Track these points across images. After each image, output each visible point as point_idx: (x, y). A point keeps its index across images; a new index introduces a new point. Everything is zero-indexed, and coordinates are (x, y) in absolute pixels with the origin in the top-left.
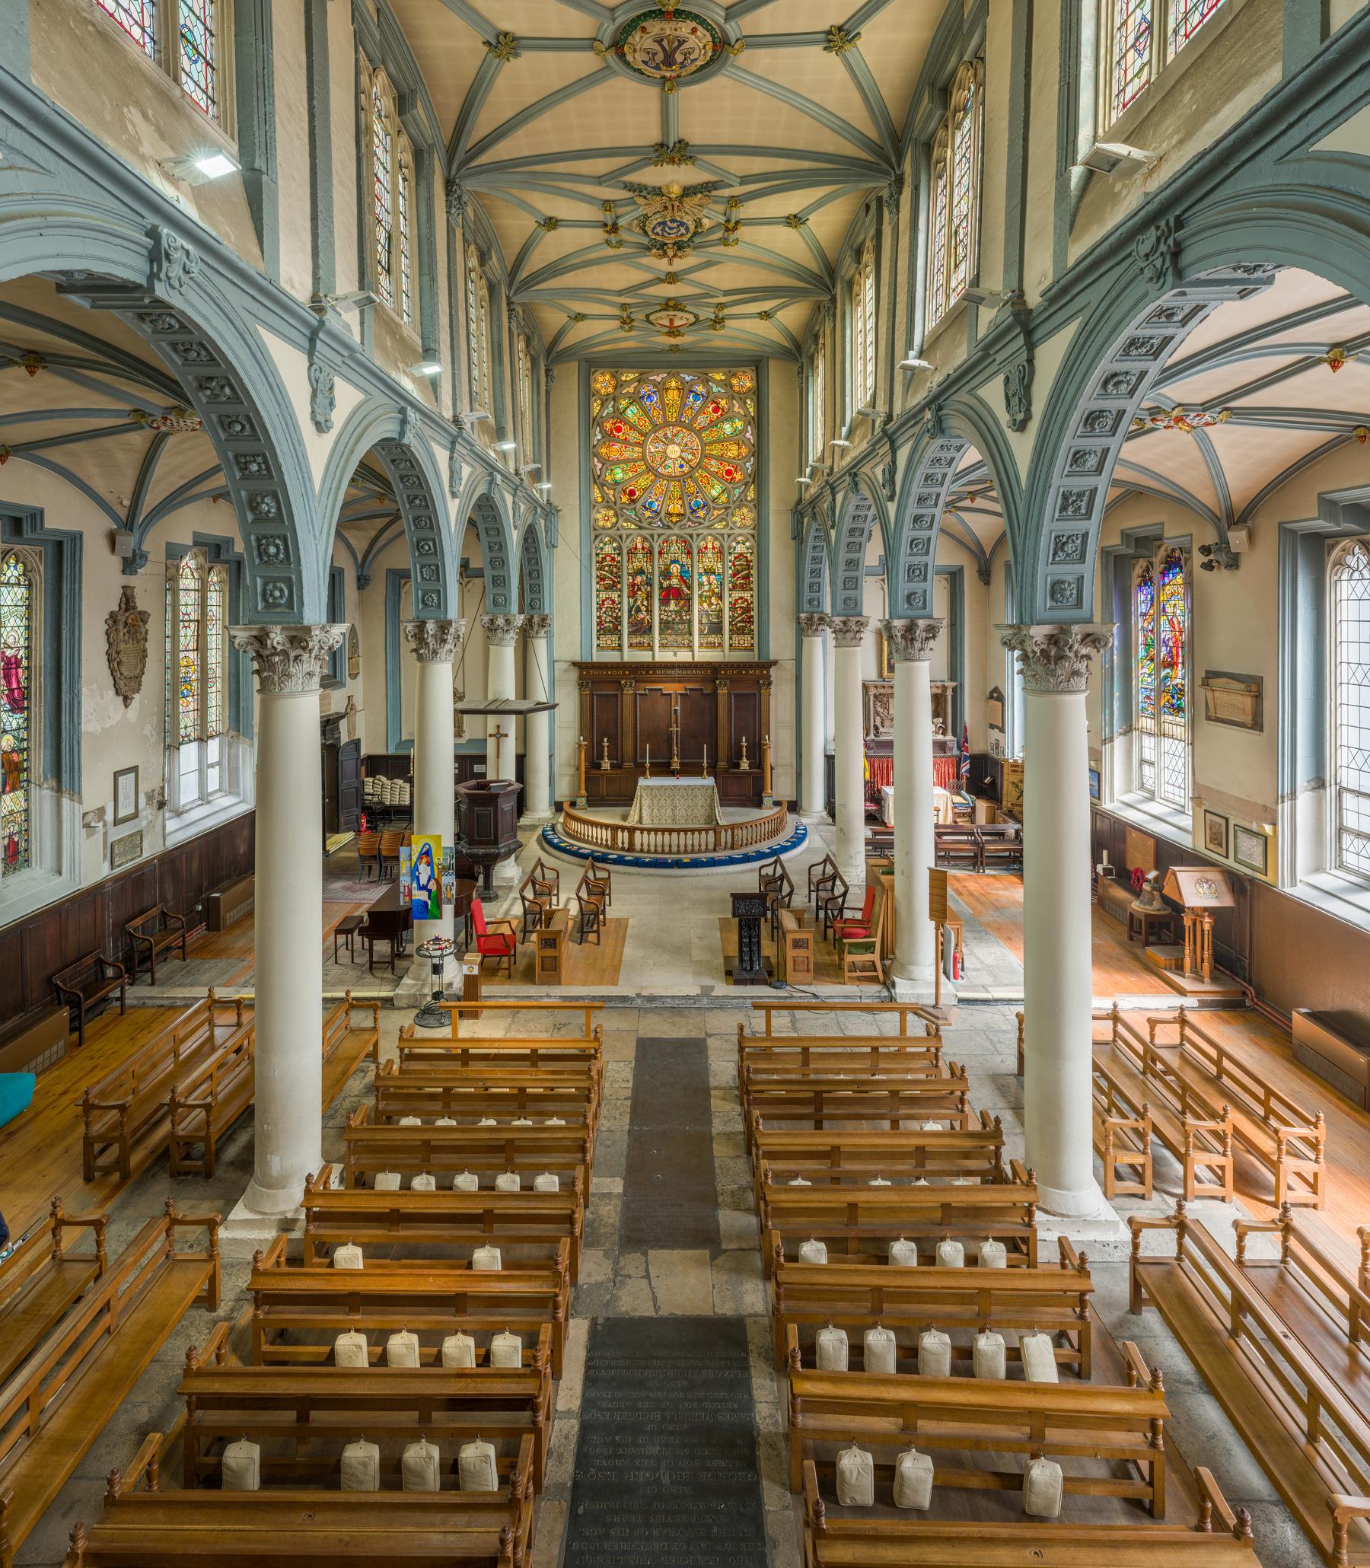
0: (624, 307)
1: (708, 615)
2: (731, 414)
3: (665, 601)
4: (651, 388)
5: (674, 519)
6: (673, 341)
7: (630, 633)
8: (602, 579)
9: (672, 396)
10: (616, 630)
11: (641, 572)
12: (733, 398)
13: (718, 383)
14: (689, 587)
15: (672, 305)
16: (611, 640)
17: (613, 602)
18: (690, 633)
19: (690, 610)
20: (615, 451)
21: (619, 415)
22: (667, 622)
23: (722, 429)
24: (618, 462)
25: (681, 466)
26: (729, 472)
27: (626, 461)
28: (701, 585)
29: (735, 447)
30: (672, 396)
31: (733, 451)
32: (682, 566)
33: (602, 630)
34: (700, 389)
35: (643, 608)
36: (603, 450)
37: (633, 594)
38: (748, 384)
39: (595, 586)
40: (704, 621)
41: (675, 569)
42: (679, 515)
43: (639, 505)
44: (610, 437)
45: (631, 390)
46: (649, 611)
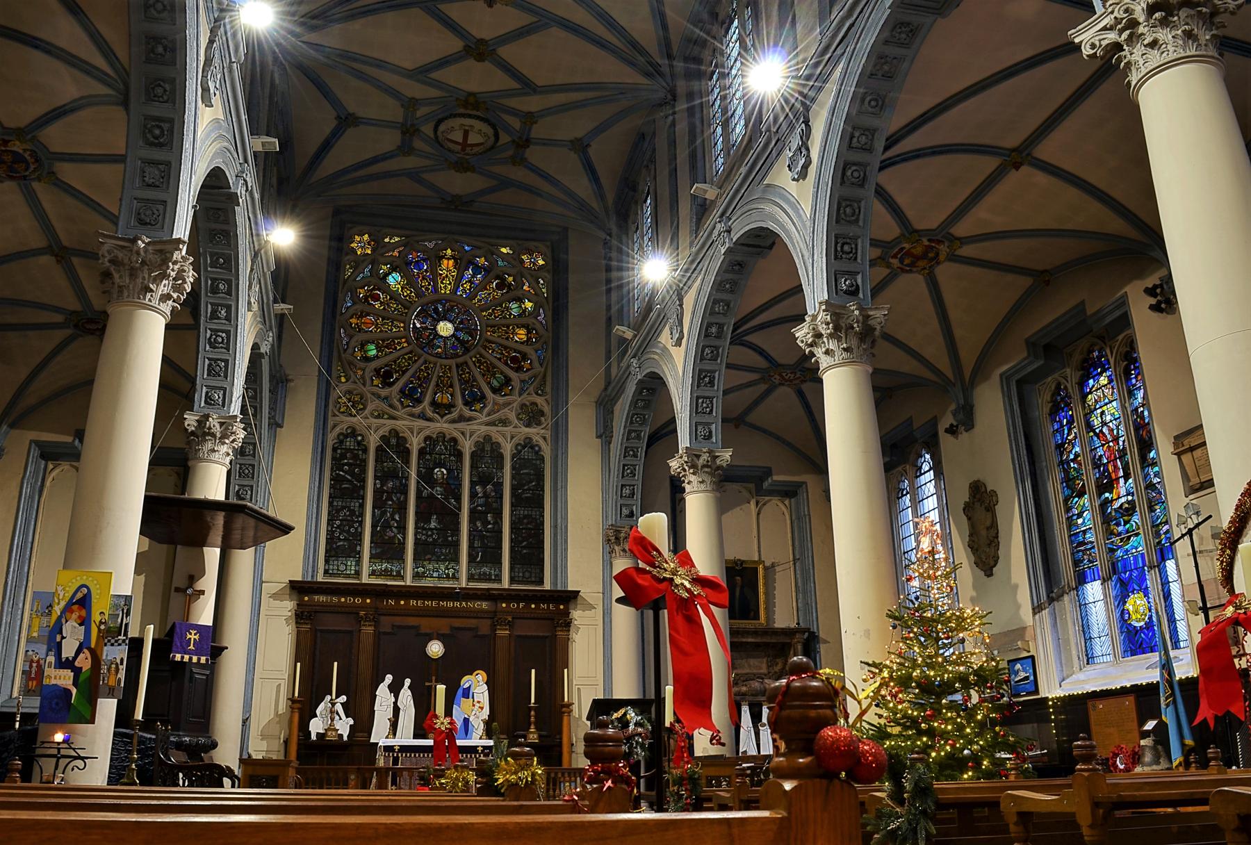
0: (411, 104)
1: (482, 538)
2: (519, 293)
3: (422, 517)
6: (460, 184)
7: (372, 557)
12: (522, 276)
14: (458, 499)
15: (472, 104)
17: (352, 512)
22: (426, 543)
23: (508, 309)
26: (514, 359)
28: (473, 495)
31: (521, 334)
34: (481, 261)
36: (354, 321)
38: (541, 262)
41: (440, 472)
42: (450, 407)
45: (396, 253)
46: (402, 528)
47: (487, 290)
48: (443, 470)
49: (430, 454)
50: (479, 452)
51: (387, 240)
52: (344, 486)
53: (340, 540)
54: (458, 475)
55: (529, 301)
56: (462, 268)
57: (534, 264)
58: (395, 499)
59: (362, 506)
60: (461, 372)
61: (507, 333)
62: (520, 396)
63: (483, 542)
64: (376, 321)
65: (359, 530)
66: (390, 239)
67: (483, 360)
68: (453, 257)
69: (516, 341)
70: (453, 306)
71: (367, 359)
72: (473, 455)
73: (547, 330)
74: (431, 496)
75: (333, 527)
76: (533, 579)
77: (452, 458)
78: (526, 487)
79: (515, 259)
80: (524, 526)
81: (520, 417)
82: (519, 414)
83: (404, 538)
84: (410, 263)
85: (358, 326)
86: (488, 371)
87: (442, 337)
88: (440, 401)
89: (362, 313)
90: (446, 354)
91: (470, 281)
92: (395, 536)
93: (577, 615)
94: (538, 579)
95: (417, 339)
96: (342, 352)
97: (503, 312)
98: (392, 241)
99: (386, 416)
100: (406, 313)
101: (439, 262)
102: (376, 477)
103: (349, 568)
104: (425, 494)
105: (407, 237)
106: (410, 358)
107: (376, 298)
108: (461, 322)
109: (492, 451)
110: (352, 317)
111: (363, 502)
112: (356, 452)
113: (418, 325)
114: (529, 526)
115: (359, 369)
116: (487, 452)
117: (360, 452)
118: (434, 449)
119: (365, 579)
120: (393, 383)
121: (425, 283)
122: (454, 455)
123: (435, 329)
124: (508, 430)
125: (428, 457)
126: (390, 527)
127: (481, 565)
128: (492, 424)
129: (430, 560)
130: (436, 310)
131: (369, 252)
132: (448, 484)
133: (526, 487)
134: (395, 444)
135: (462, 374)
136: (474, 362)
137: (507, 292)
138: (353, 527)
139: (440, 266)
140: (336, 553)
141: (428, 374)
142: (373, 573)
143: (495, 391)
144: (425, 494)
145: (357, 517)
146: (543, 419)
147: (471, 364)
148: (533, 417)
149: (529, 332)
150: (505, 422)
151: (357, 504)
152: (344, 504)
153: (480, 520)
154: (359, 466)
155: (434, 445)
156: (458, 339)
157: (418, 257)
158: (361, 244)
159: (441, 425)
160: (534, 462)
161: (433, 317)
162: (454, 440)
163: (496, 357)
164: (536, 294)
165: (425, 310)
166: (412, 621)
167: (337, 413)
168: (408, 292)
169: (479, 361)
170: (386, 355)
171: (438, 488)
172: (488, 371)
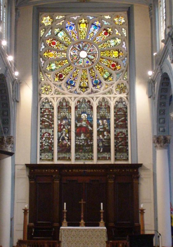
1: (103, 142)
2: (114, 36)
3: (78, 134)
4: (72, 23)
7: (58, 152)
8: (43, 122)
9: (83, 27)
10: (50, 150)
11: (65, 118)
13: (107, 20)
14: (92, 126)
16: (46, 155)
17: (50, 134)
18: (92, 151)
19: (92, 140)
20: (52, 55)
21: (55, 37)
22: (79, 146)
23: (109, 43)
24: (52, 61)
25: (87, 62)
26: (113, 65)
27: (58, 60)
28: (98, 125)
29: (117, 52)
30: (83, 27)
31: (115, 54)
32: (88, 115)
33: (43, 151)
34: (97, 23)
35: (66, 138)
36: (45, 54)
37: (60, 130)
38: (123, 21)
39: (39, 126)
40: (101, 145)
41: (84, 116)
42: (87, 88)
43: (64, 82)
44: (49, 49)
45: (61, 24)
46: (69, 139)
47: (100, 35)
48: (85, 115)
49: (80, 108)
50: (100, 106)
51: (57, 18)
52: (45, 124)
53: (45, 146)
54: (91, 116)
55: (119, 39)
56: (89, 27)
57: (120, 22)
58: (66, 128)
59: (53, 131)
60: (91, 73)
61: (109, 54)
63: (103, 144)
64: (55, 53)
65: (53, 141)
66: (58, 17)
67: (100, 67)
68: (85, 23)
69: (114, 57)
70: (86, 44)
71: (52, 70)
72: (98, 107)
73: (126, 51)
74: (81, 126)
75: (42, 140)
76: (124, 158)
77: (89, 109)
78: (120, 120)
79: (112, 21)
80: (120, 136)
81: (117, 90)
82: (116, 89)
83: (71, 144)
84: (67, 27)
85: (48, 56)
86: (102, 71)
87: (82, 58)
88: (83, 86)
90: (84, 65)
91: (93, 33)
92: (67, 143)
93: (142, 173)
94: (126, 158)
95: (72, 60)
97: (107, 45)
98: (59, 18)
99: (61, 94)
100: (67, 49)
102: (58, 119)
103: (49, 157)
104: (78, 125)
105: (65, 16)
106: (69, 68)
107: (54, 44)
108: (90, 51)
109: (105, 105)
110: (45, 53)
111: (54, 130)
112: (49, 109)
113: (72, 54)
114: (122, 136)
116: (104, 106)
117: (51, 109)
118: (81, 106)
119: (56, 162)
120: (63, 79)
121: (74, 35)
122: (90, 108)
123: (79, 55)
124: (112, 96)
125: (79, 109)
126: (64, 139)
127: (102, 153)
128: (105, 94)
129: (81, 152)
130: (79, 47)
131: (50, 24)
132: (88, 120)
133: (120, 120)
134: (64, 106)
135: (91, 73)
136: (96, 68)
137: (109, 36)
138: (50, 140)
139: (80, 27)
140: (44, 151)
141: (77, 75)
142: (59, 159)
143: (106, 79)
144: (78, 125)
145: (51, 136)
147: (94, 68)
148: (122, 90)
149: (119, 53)
150: (110, 92)
151: (51, 131)
152: (46, 131)
153: (101, 134)
154: (51, 115)
155: (81, 105)
156: (89, 58)
157: (70, 24)
158: (46, 20)
159: (84, 95)
160: (123, 109)
161: (78, 50)
162: (89, 101)
163: (105, 65)
164: (121, 36)
165: (74, 47)
166: (75, 178)
169: (98, 67)
170: (59, 68)
171: (84, 123)
172: (102, 71)
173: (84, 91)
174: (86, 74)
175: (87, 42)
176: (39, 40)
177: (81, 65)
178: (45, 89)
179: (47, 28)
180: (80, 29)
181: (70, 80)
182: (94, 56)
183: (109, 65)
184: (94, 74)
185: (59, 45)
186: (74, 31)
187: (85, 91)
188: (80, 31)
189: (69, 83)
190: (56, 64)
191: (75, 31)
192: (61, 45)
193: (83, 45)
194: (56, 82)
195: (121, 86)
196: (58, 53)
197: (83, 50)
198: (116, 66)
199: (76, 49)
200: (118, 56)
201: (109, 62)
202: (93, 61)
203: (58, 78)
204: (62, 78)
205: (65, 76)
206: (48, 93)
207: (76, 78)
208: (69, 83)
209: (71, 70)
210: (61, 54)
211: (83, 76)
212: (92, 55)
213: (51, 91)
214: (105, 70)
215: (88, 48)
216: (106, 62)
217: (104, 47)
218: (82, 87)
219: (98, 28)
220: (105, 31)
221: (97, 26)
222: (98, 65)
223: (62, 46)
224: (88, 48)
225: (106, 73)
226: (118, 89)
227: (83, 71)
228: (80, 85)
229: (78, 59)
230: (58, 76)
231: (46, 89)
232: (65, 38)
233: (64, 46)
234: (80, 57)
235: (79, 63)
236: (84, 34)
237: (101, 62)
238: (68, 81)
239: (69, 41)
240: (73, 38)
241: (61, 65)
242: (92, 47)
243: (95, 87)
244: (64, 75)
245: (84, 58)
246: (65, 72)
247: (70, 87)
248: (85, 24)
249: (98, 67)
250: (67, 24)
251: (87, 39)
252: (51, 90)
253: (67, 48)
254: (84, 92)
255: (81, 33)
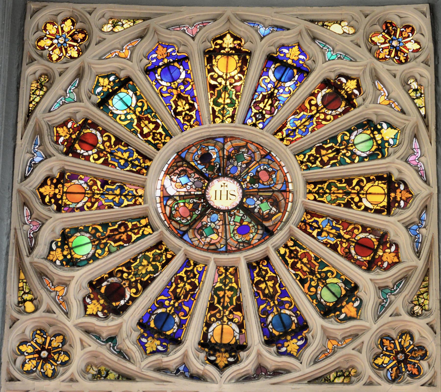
5: (222, 359)
36: (48, 190)
47: (305, 110)
60: (257, 279)
61: (347, 194)
62: (376, 321)
64: (90, 187)
66: (114, 26)
69: (366, 209)
81: (379, 361)
82: (377, 356)
85: (57, 201)
86: (312, 273)
87: (218, 211)
89: (62, 174)
90: (226, 244)
96: (25, 252)
97: (338, 151)
99: (112, 375)
101: (210, 61)
108: (255, 179)
110: (44, 184)
115: (59, 284)
120: (125, 308)
123: (203, 196)
135: (259, 282)
146: (424, 364)
156: (249, 212)
157: (169, 56)
167: (17, 375)
168: (152, 126)
172: (312, 273)
173: (222, 364)
174: (234, 285)
175: (242, 140)
176: (20, 125)
177: (210, 244)
178: (39, 352)
179: (60, 74)
180: (212, 77)
181: (159, 311)
182: (275, 203)
183: (344, 245)
184: (270, 284)
185: (114, 148)
186: (182, 87)
187: (229, 364)
188: (213, 87)
189: (152, 325)
190: (94, 235)
191: (189, 88)
192: (123, 152)
193: (223, 149)
194: (93, 320)
195: (401, 346)
196: (106, 187)
197: (225, 175)
198: (375, 251)
199: (192, 168)
200: (385, 203)
201: (342, 233)
202: (267, 224)
203: (102, 301)
204: (122, 302)
205: (134, 290)
206: (50, 373)
207: (189, 304)
208: (152, 325)
209: (163, 266)
210: (122, 188)
211: (221, 293)
212: (267, 199)
213: (64, 364)
214: (326, 269)
215: (248, 164)
216: (328, 233)
217: (322, 162)
218: (216, 344)
219: (297, 77)
220: (326, 91)
221: (291, 67)
222: (290, 244)
223: (126, 155)
224: (248, 164)
225: (328, 281)
226: (387, 360)
227: (222, 270)
228: (205, 335)
229: (198, 212)
230: (103, 290)
231: (44, 354)
232: (139, 119)
233: (136, 155)
234: (210, 207)
235: (206, 232)
236: (232, 104)
237: (305, 231)
238: (151, 313)
239: (160, 130)
240: (180, 118)
241: (120, 240)
242: (265, 161)
243: (274, 349)
244: (130, 287)
245: (229, 211)
246: (135, 275)
247: (158, 342)
248: (236, 57)
249: (291, 251)
250: (154, 56)
251: (244, 123)
252: (67, 358)
253: (148, 163)
254: (221, 369)
255: (219, 96)
